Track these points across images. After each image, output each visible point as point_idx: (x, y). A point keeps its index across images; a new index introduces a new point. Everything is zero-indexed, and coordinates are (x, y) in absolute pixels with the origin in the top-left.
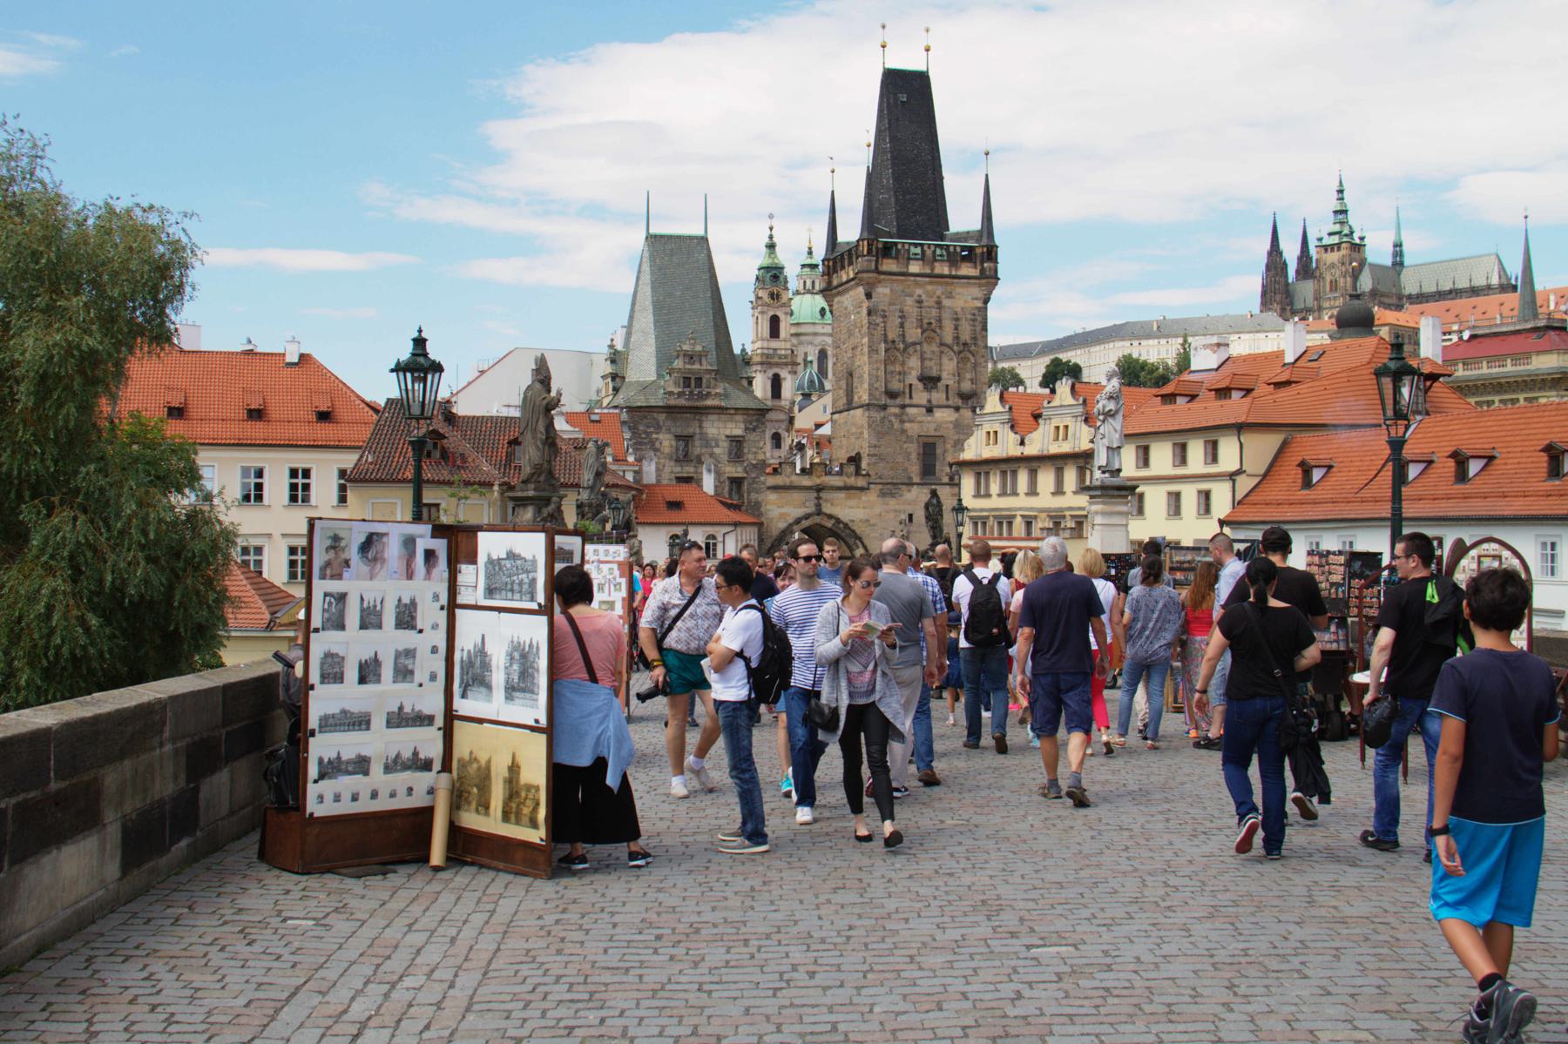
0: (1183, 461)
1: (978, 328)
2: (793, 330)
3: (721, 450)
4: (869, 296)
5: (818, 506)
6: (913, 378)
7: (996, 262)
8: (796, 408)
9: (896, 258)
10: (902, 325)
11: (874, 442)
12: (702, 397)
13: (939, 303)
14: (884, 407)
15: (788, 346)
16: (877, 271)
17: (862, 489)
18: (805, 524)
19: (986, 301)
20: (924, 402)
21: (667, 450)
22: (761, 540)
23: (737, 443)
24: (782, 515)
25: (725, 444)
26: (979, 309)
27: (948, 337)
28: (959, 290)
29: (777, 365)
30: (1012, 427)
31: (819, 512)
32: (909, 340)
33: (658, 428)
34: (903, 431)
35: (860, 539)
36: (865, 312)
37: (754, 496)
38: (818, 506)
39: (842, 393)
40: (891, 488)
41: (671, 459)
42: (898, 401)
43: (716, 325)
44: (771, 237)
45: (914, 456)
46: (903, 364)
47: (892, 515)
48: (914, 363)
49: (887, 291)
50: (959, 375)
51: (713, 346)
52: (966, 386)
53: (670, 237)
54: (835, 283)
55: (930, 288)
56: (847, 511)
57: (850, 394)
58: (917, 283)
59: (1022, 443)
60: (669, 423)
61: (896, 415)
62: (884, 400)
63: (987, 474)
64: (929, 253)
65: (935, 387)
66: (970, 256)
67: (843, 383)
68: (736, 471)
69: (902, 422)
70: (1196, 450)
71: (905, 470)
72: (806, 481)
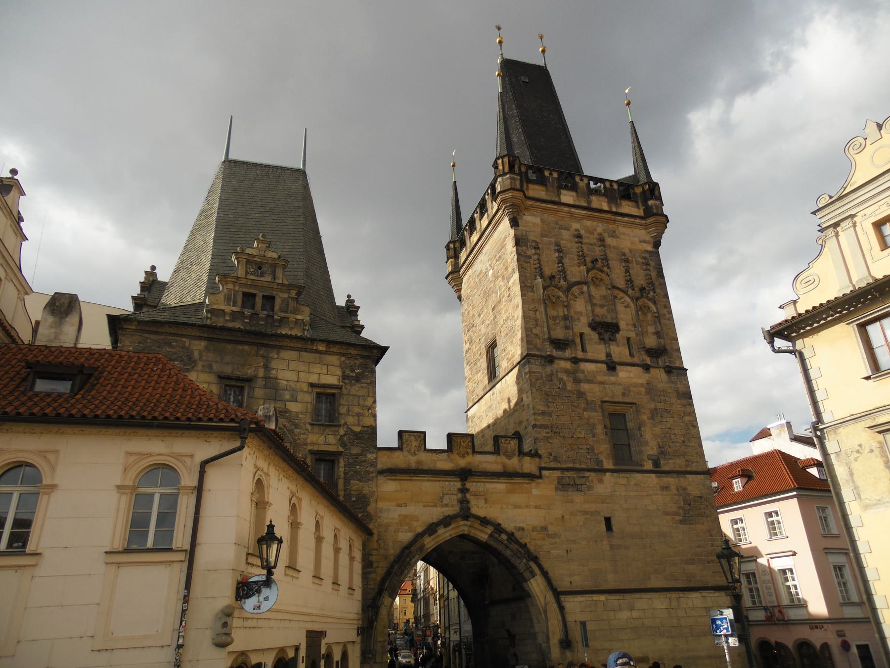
1: (654, 274)
3: (300, 406)
4: (514, 223)
5: (464, 503)
6: (582, 326)
7: (660, 198)
9: (545, 185)
10: (560, 261)
11: (542, 408)
13: (602, 240)
14: (551, 360)
17: (530, 477)
18: (445, 534)
19: (657, 244)
20: (603, 357)
22: (367, 565)
23: (327, 398)
24: (405, 520)
26: (650, 253)
27: (618, 276)
28: (622, 229)
31: (465, 513)
34: (581, 394)
35: (535, 559)
37: (355, 485)
38: (464, 503)
40: (573, 479)
42: (568, 353)
45: (599, 429)
46: (568, 306)
48: (580, 306)
49: (537, 220)
52: (651, 341)
55: (588, 223)
58: (572, 216)
60: (211, 356)
61: (567, 371)
62: (549, 350)
65: (612, 339)
68: (327, 441)
71: (591, 449)
72: (444, 464)
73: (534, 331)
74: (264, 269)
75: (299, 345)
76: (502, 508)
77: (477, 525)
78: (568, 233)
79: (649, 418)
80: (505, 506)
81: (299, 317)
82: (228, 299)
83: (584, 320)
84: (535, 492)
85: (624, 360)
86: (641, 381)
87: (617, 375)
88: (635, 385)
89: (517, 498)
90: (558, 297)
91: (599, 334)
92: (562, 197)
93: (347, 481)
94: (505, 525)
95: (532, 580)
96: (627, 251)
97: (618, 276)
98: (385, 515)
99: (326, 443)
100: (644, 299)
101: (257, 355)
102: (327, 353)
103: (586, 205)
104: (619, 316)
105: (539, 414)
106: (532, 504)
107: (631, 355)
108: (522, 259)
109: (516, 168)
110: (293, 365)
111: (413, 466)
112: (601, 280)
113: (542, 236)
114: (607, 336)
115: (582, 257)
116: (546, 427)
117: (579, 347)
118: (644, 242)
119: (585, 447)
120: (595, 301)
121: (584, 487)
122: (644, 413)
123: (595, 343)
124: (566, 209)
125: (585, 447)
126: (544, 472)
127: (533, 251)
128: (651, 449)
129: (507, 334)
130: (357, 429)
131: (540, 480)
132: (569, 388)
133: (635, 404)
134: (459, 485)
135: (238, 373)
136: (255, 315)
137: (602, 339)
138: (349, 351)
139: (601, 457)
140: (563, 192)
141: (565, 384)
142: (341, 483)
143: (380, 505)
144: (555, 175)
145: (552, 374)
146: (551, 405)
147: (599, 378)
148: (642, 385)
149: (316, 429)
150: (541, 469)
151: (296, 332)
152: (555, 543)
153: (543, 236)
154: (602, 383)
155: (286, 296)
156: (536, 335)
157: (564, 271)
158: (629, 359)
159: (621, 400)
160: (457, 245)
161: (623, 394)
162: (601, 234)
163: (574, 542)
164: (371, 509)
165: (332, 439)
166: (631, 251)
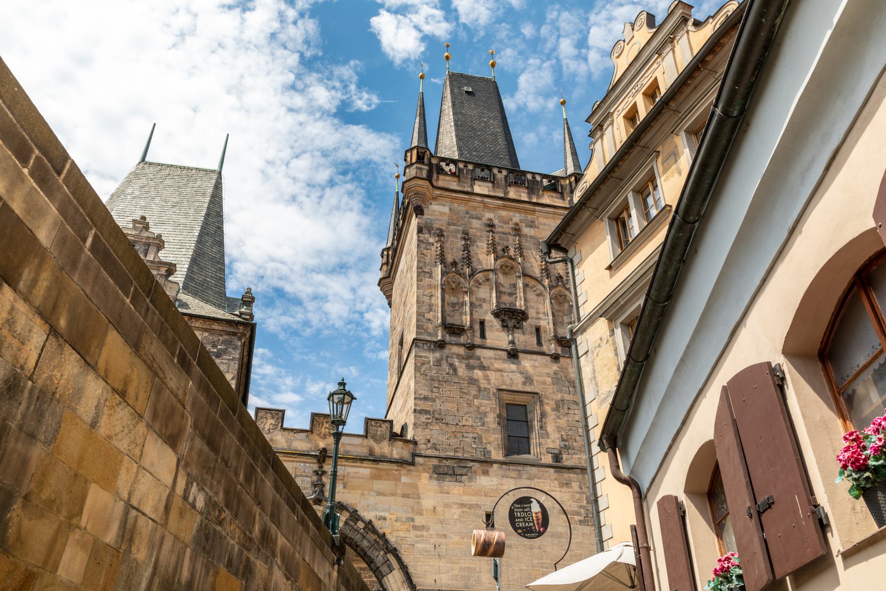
10: (466, 248)
11: (425, 392)
13: (517, 230)
16: (429, 179)
17: (401, 462)
34: (473, 381)
35: (395, 552)
42: (462, 339)
47: (456, 512)
49: (446, 210)
55: (503, 213)
56: (372, 499)
61: (459, 356)
65: (518, 327)
69: (470, 367)
71: (478, 439)
73: (427, 316)
76: (362, 494)
78: (479, 222)
79: (553, 410)
80: (366, 492)
84: (404, 479)
85: (529, 348)
86: (547, 370)
87: (519, 363)
89: (379, 485)
90: (459, 284)
91: (503, 321)
95: (390, 576)
105: (420, 399)
106: (399, 491)
107: (539, 343)
108: (423, 245)
109: (426, 160)
112: (512, 268)
113: (449, 224)
114: (511, 324)
116: (426, 412)
117: (478, 334)
119: (471, 435)
120: (502, 289)
121: (464, 478)
122: (547, 404)
123: (497, 330)
124: (478, 198)
125: (471, 435)
127: (437, 239)
128: (553, 441)
131: (412, 468)
133: (537, 393)
134: (315, 467)
137: (505, 326)
138: (213, 326)
139: (489, 447)
140: (476, 182)
141: (455, 370)
145: (441, 359)
146: (435, 390)
147: (498, 365)
148: (548, 375)
150: (414, 455)
152: (422, 536)
153: (449, 224)
158: (536, 348)
159: (522, 390)
160: (390, 253)
161: (524, 383)
162: (517, 224)
163: (445, 536)
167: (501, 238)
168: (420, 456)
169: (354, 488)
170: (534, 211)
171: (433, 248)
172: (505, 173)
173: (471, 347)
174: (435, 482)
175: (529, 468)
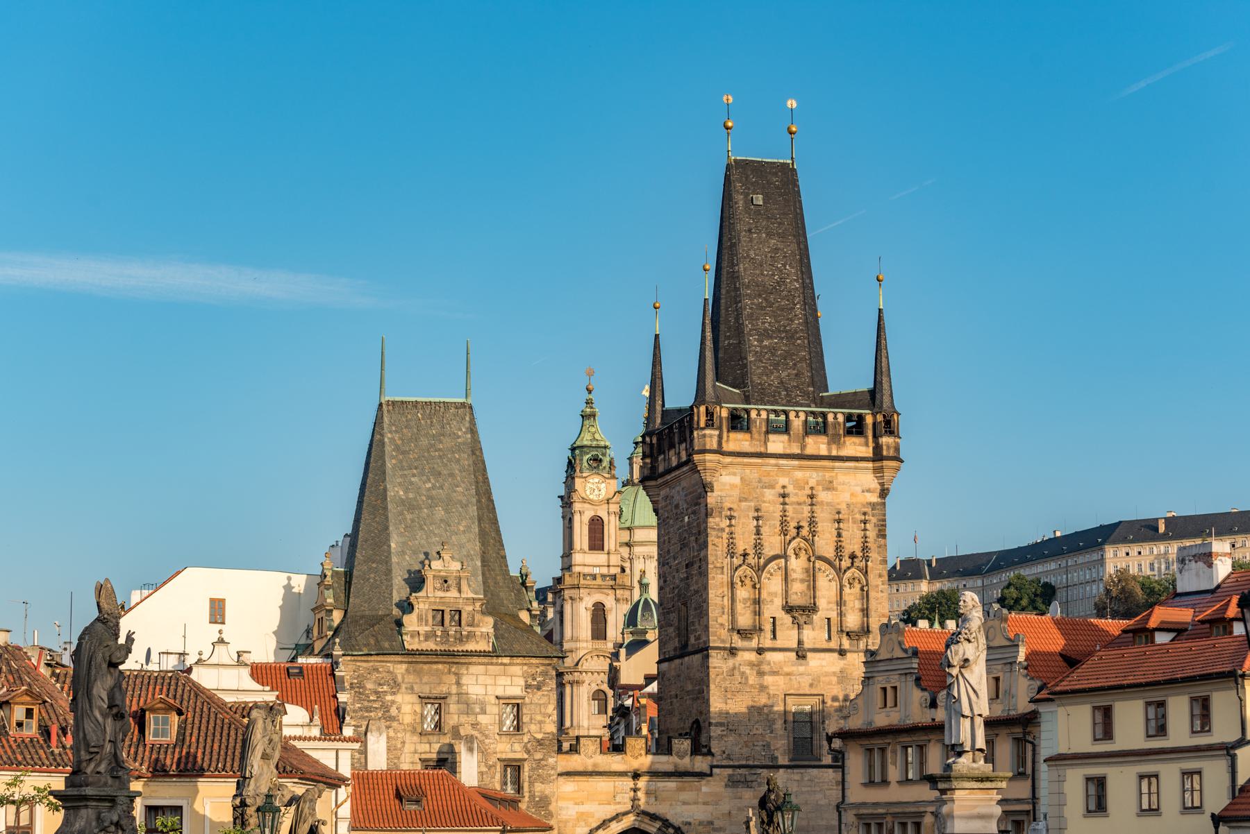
0: (1162, 730)
1: (872, 534)
2: (625, 537)
6: (773, 608)
8: (623, 651)
9: (748, 430)
10: (758, 533)
12: (460, 639)
13: (812, 497)
14: (733, 651)
15: (615, 560)
17: (701, 775)
20: (795, 646)
21: (408, 719)
24: (582, 817)
25: (493, 709)
26: (873, 506)
27: (825, 545)
29: (600, 588)
30: (918, 680)
32: (769, 551)
33: (395, 686)
34: (763, 688)
36: (703, 510)
38: (634, 799)
39: (671, 630)
41: (414, 731)
42: (754, 643)
43: (483, 535)
44: (589, 403)
48: (773, 585)
49: (736, 480)
50: (841, 602)
51: (479, 563)
52: (853, 620)
53: (415, 404)
54: (661, 469)
55: (799, 474)
56: (680, 809)
57: (684, 631)
59: (933, 705)
60: (411, 678)
61: (751, 664)
63: (883, 750)
64: (797, 423)
66: (856, 428)
67: (673, 616)
68: (510, 749)
69: (761, 674)
70: (1179, 708)
71: (767, 746)
73: (720, 620)
74: (450, 582)
75: (486, 660)
77: (647, 820)
78: (772, 491)
81: (484, 630)
82: (420, 618)
83: (779, 602)
84: (704, 789)
87: (807, 664)
88: (827, 674)
89: (685, 796)
91: (794, 617)
92: (769, 444)
93: (531, 783)
94: (672, 820)
96: (843, 507)
97: (825, 545)
98: (564, 812)
99: (513, 751)
100: (853, 570)
101: (450, 672)
102: (510, 664)
103: (799, 451)
104: (818, 594)
107: (830, 638)
110: (481, 679)
111: (590, 769)
114: (802, 619)
115: (784, 522)
117: (769, 635)
118: (869, 491)
120: (794, 576)
123: (788, 628)
124: (773, 461)
126: (716, 771)
129: (696, 609)
130: (539, 736)
132: (751, 682)
135: (437, 691)
136: (446, 633)
139: (777, 754)
140: (771, 437)
141: (747, 678)
142: (526, 785)
143: (560, 804)
144: (764, 415)
145: (734, 668)
147: (786, 669)
148: (834, 673)
149: (504, 738)
150: (712, 767)
151: (483, 646)
154: (788, 674)
155: (470, 608)
156: (722, 625)
157: (758, 546)
158: (825, 646)
160: (655, 440)
161: (811, 685)
162: (812, 488)
164: (551, 808)
165: (517, 747)
166: (848, 505)
167: (796, 512)
168: (717, 767)
169: (664, 800)
170: (833, 468)
171: (725, 535)
172: (802, 416)
173: (760, 651)
174: (729, 790)
175: (810, 770)
